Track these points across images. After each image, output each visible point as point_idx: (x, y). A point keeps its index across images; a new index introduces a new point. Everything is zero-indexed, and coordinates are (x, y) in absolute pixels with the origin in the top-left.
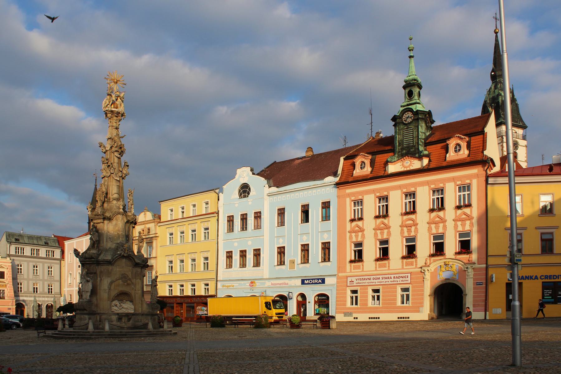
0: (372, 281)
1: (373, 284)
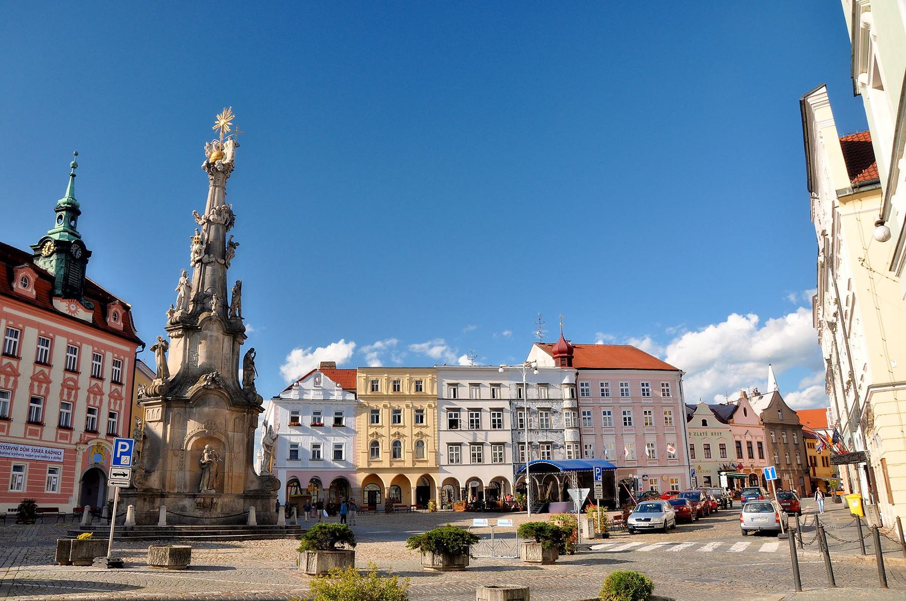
0: (19, 452)
1: (20, 457)
